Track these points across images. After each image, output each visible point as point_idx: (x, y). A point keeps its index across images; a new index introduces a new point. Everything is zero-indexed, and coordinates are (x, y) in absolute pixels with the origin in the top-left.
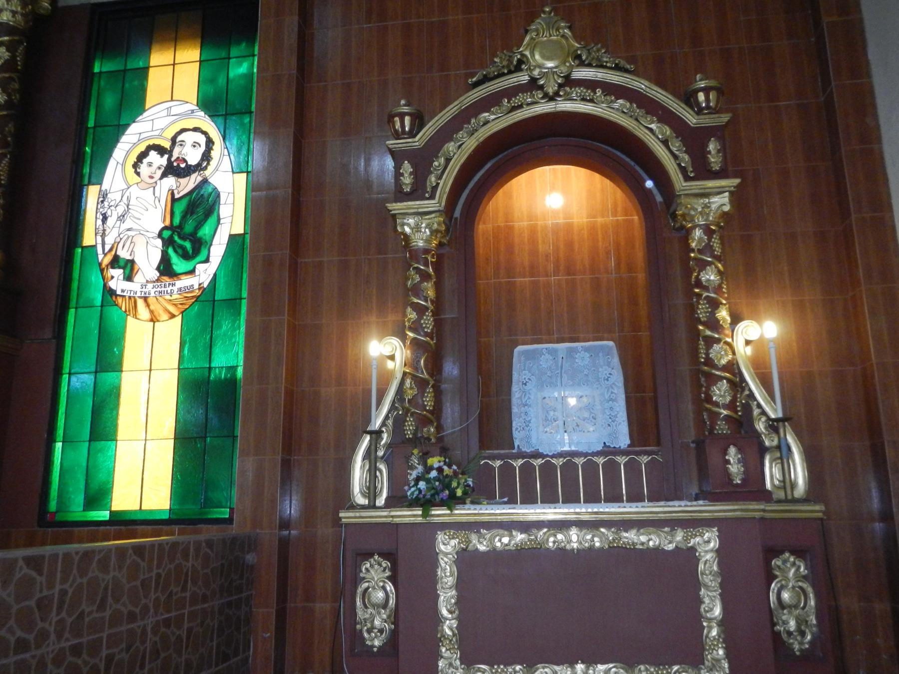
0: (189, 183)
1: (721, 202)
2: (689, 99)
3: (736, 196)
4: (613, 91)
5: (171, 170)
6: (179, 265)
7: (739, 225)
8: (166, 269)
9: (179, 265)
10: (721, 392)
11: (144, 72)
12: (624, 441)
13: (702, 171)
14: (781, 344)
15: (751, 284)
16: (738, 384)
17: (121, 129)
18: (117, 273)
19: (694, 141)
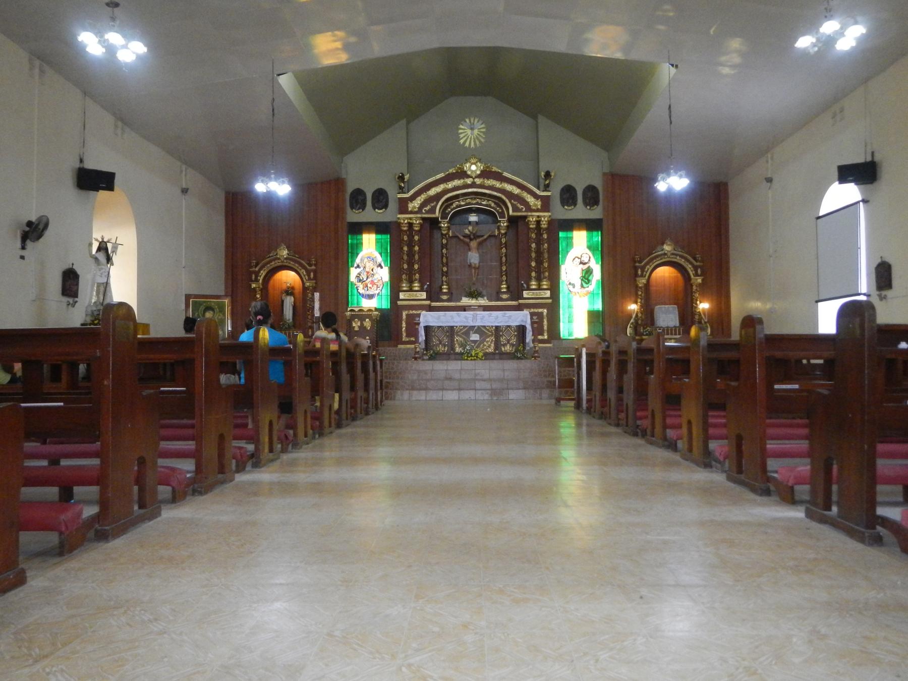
0: (586, 267)
1: (699, 281)
2: (695, 259)
3: (703, 280)
4: (682, 257)
5: (581, 263)
6: (585, 285)
7: (702, 286)
8: (582, 286)
9: (585, 285)
10: (697, 317)
11: (572, 238)
12: (678, 325)
13: (696, 275)
14: (708, 310)
15: (704, 297)
16: (700, 315)
17: (568, 252)
18: (571, 287)
19: (695, 268)
